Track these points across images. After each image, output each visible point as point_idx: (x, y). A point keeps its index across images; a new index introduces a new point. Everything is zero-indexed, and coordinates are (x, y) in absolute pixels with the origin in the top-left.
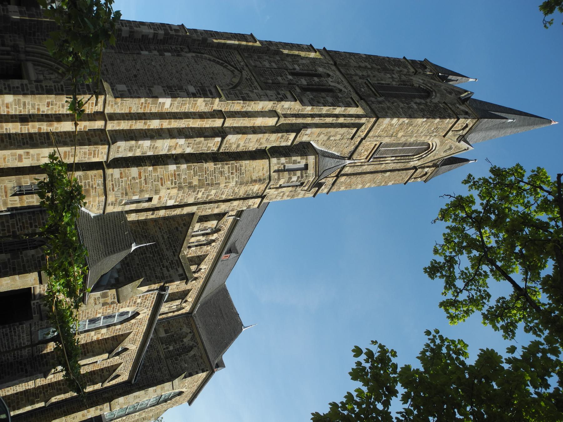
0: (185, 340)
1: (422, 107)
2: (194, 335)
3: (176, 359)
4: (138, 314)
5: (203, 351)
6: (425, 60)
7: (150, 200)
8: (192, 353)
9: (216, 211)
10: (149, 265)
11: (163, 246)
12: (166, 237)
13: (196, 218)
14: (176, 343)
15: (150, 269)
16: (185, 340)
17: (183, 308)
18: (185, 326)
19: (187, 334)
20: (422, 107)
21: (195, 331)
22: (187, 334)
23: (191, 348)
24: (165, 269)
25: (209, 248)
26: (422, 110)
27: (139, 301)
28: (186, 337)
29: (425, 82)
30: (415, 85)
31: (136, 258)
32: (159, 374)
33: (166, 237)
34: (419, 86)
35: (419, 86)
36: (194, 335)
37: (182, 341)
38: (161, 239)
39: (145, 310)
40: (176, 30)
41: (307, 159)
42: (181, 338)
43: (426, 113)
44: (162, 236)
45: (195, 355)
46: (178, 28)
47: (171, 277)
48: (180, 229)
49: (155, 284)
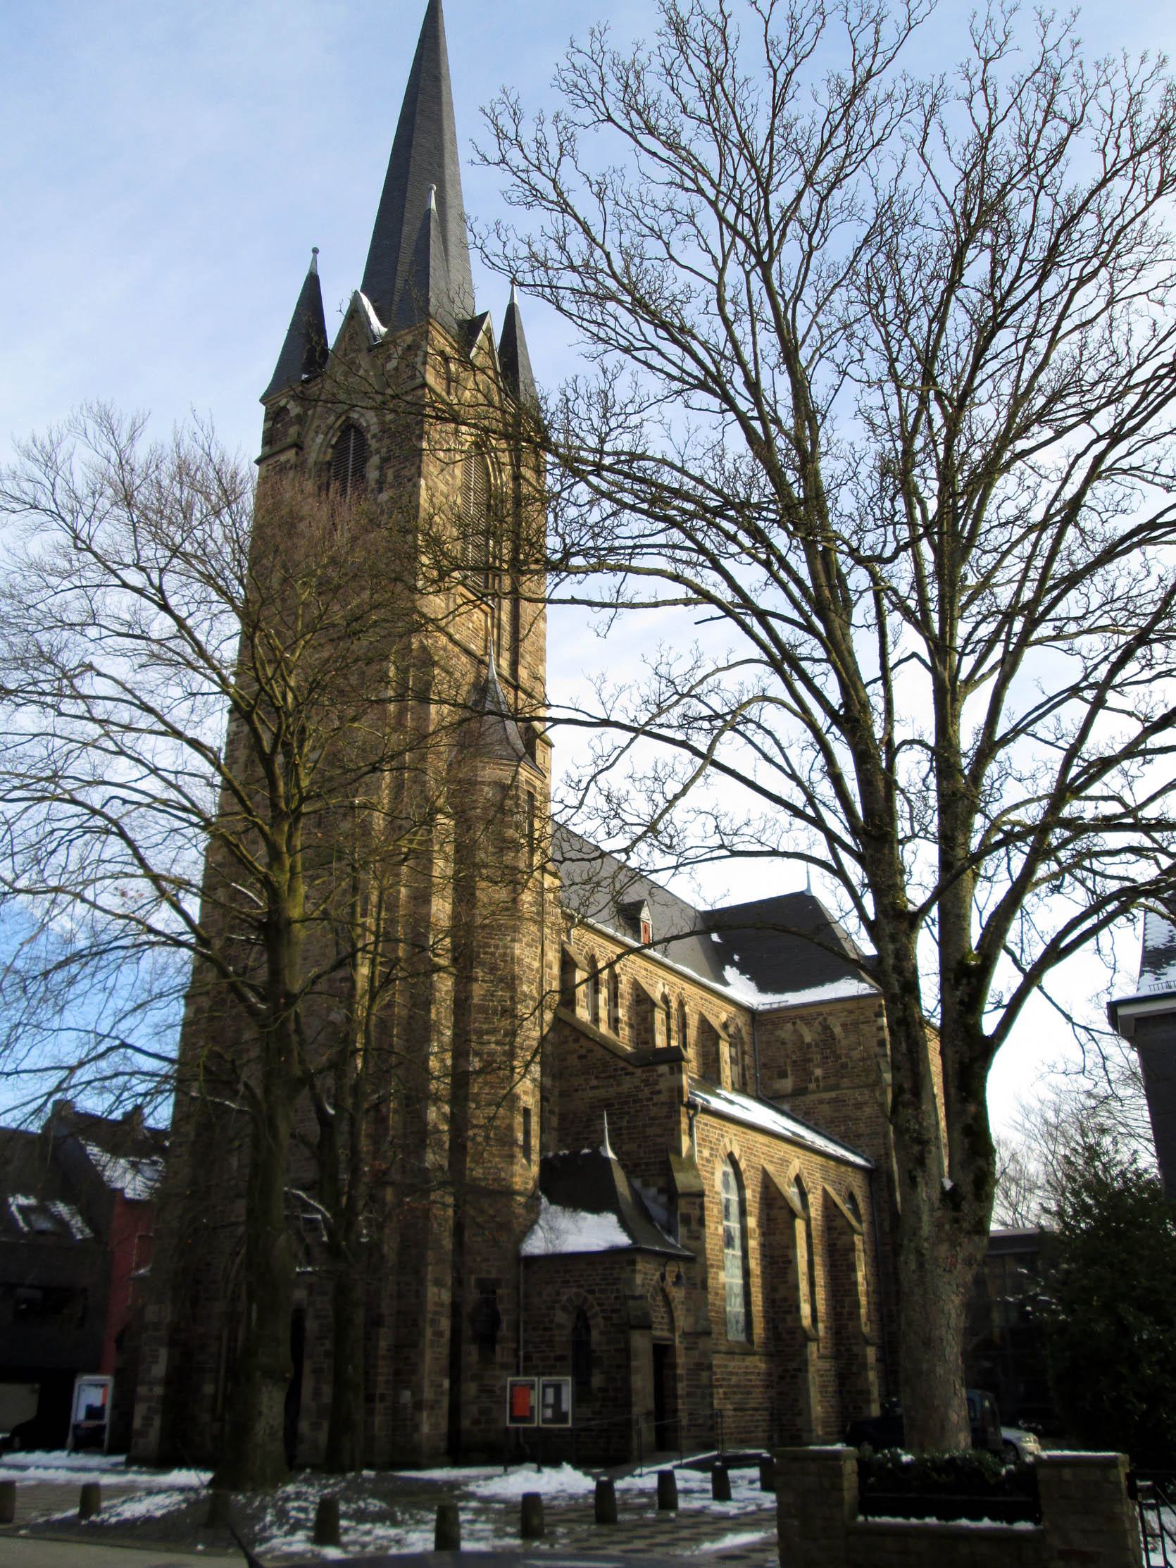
0: (808, 1039)
1: (390, 474)
2: (802, 1018)
3: (844, 1066)
4: (731, 1156)
5: (839, 1006)
6: (264, 400)
7: (527, 1112)
8: (838, 1030)
9: (556, 970)
10: (645, 1126)
11: (612, 1091)
12: (594, 1082)
13: (564, 1013)
14: (810, 1060)
15: (651, 1125)
16: (808, 1039)
17: (739, 1030)
18: (778, 1033)
19: (795, 1031)
20: (390, 474)
21: (793, 1014)
22: (795, 1031)
23: (826, 1028)
24: (655, 1098)
25: (624, 978)
26: (399, 481)
27: (706, 1153)
28: (801, 1036)
29: (323, 428)
30: (328, 458)
31: (625, 1148)
32: (868, 1110)
33: (594, 1082)
34: (333, 447)
35: (333, 447)
36: (802, 1018)
37: (809, 1045)
38: (596, 1093)
39: (727, 1140)
40: (199, 1011)
41: (483, 783)
42: (804, 1047)
43: (406, 473)
44: (593, 1088)
45: (844, 1025)
46: (193, 1008)
47: (671, 1090)
48: (583, 1051)
49: (679, 1122)
